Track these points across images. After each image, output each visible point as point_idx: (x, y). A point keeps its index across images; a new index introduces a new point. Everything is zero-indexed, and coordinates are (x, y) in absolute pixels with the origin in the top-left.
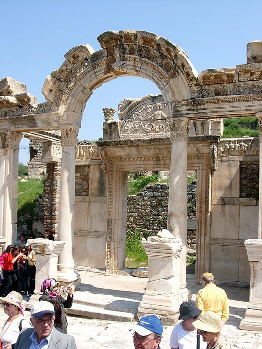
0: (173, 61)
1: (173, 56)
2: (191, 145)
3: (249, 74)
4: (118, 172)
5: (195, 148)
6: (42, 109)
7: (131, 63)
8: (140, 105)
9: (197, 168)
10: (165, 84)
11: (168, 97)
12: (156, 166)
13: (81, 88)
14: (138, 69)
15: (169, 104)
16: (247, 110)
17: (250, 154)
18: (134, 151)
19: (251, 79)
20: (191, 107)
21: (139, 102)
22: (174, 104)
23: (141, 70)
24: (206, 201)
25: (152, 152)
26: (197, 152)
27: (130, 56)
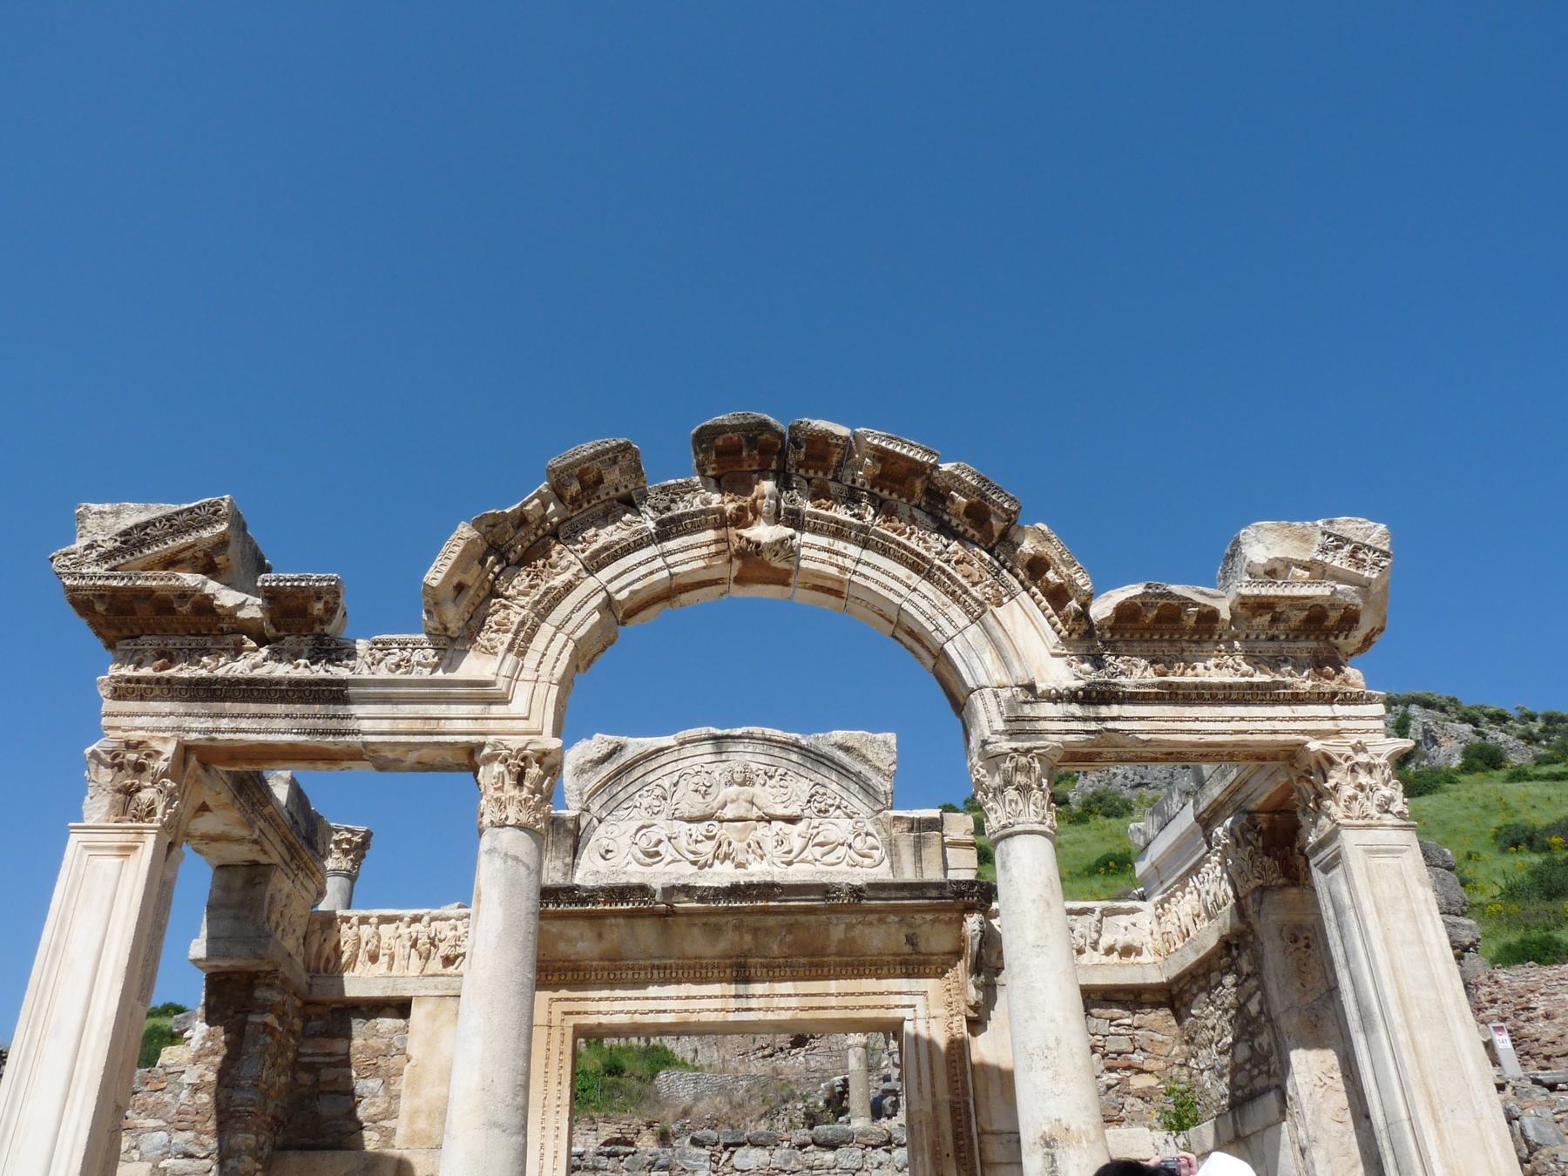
0: (990, 552)
1: (996, 534)
2: (892, 918)
3: (1268, 617)
4: (556, 1033)
5: (905, 930)
6: (395, 659)
7: (823, 541)
8: (663, 760)
9: (907, 1013)
10: (962, 620)
11: (980, 672)
12: (733, 1004)
13: (598, 599)
14: (849, 563)
15: (986, 692)
16: (1275, 732)
17: (1096, 961)
18: (647, 932)
19: (1274, 631)
20: (1075, 709)
21: (660, 751)
22: (1005, 694)
23: (860, 568)
24: (958, 1149)
25: (723, 944)
26: (907, 949)
27: (823, 512)
